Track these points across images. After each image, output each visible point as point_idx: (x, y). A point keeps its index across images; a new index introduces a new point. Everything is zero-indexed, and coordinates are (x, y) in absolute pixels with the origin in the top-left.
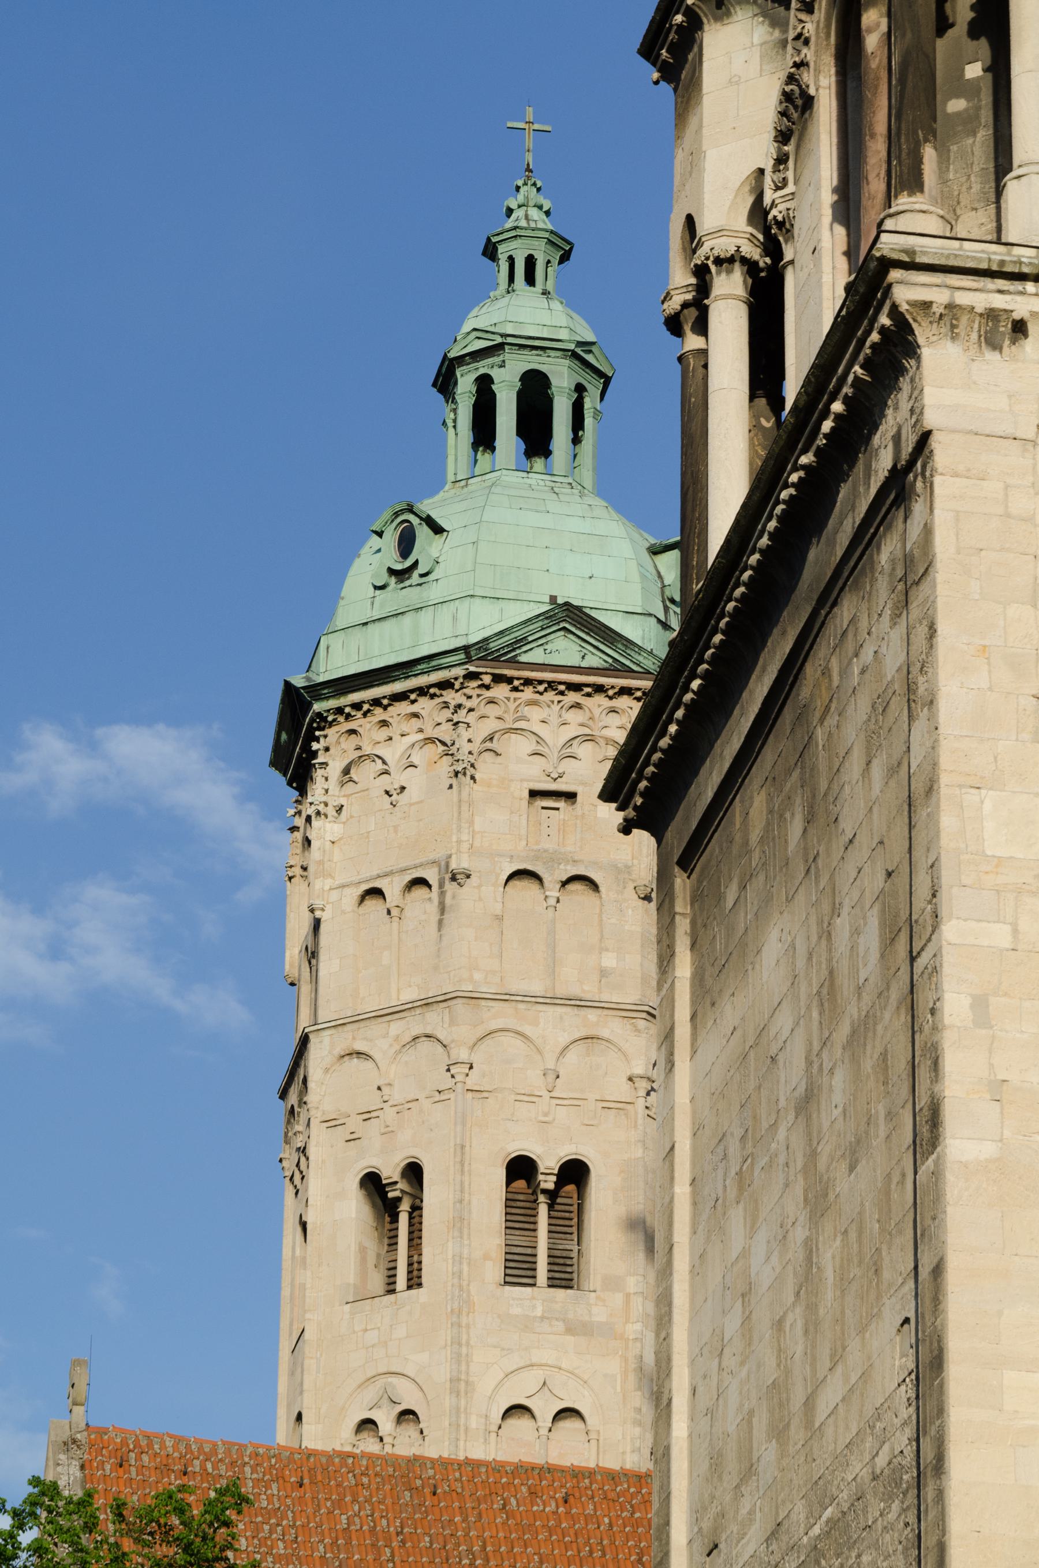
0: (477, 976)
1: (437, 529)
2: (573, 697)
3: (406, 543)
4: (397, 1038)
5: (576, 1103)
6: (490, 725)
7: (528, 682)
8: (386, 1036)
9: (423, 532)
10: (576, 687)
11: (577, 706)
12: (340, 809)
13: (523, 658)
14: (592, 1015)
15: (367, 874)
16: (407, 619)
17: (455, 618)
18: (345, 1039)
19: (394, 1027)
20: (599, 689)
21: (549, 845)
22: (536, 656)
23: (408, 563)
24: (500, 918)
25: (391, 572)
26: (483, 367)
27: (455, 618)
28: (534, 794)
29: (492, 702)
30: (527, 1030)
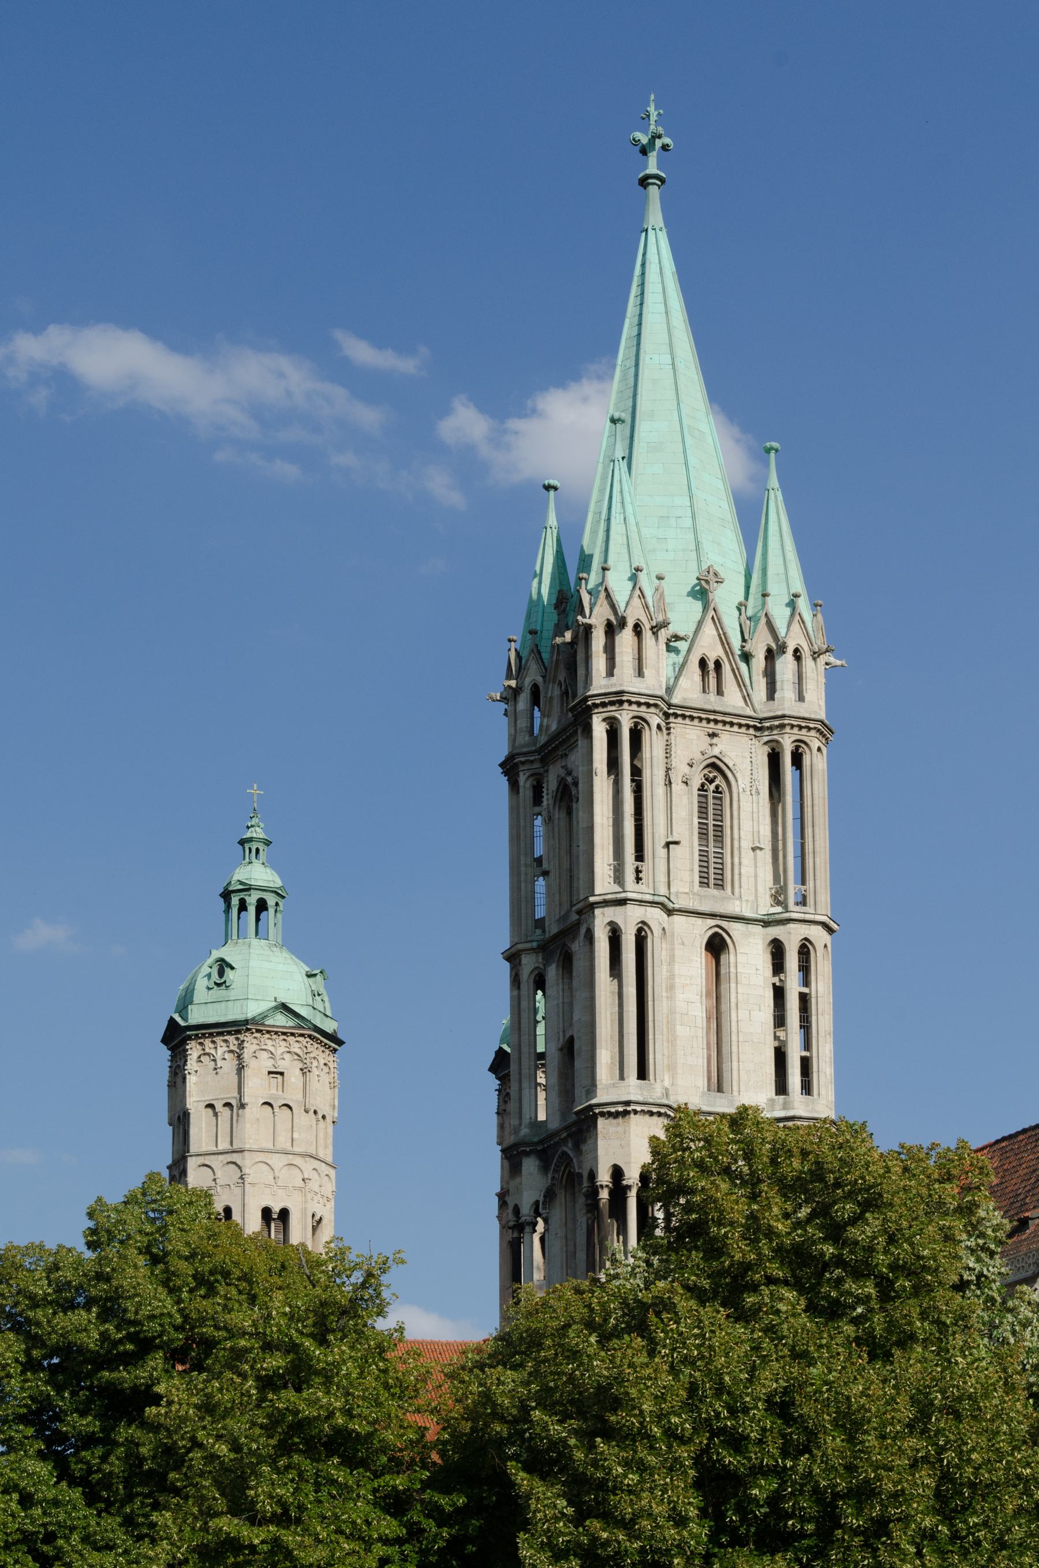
0: (251, 1141)
1: (232, 968)
2: (285, 1037)
3: (221, 973)
4: (222, 1161)
5: (285, 1187)
6: (255, 1047)
7: (268, 1032)
8: (217, 1160)
9: (227, 970)
10: (284, 1034)
11: (284, 1040)
12: (196, 1072)
13: (266, 1023)
14: (291, 1156)
15: (208, 1098)
16: (223, 1004)
17: (242, 1007)
18: (201, 1160)
19: (221, 1157)
20: (293, 1034)
21: (273, 1091)
22: (269, 1022)
23: (222, 981)
24: (258, 1120)
25: (216, 983)
26: (242, 895)
27: (242, 1007)
28: (270, 1073)
29: (255, 1038)
30: (269, 1162)
